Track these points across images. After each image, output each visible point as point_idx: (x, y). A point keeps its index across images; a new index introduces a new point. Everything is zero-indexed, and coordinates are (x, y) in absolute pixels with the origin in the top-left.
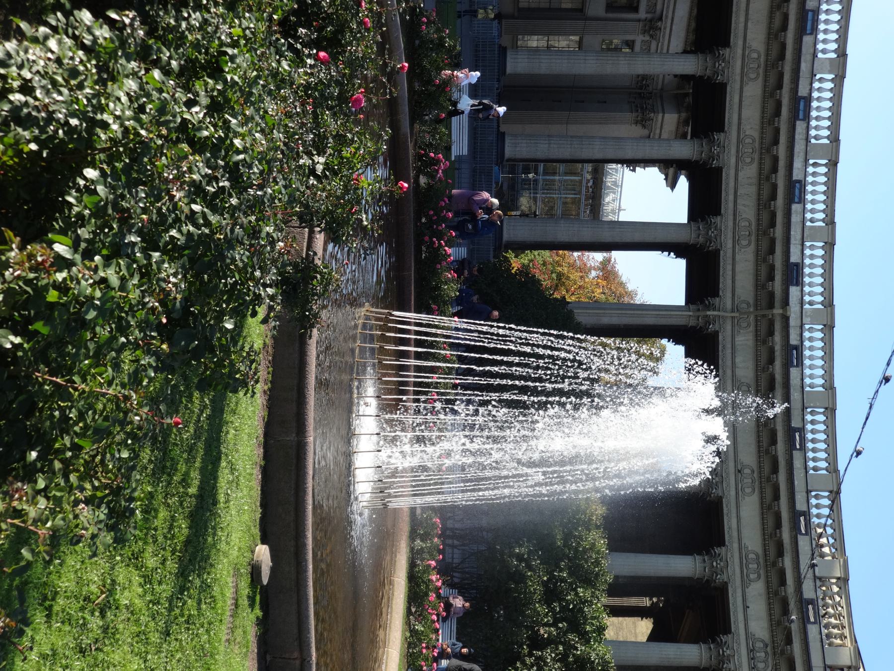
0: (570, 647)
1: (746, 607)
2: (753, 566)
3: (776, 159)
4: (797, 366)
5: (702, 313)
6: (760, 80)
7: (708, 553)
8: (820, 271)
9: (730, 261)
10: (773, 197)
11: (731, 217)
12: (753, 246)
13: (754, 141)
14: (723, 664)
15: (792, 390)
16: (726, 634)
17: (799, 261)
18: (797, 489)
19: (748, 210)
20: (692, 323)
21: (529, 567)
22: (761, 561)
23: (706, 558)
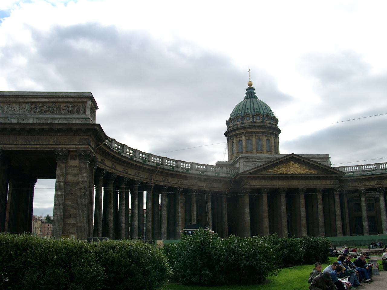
6: (383, 180)
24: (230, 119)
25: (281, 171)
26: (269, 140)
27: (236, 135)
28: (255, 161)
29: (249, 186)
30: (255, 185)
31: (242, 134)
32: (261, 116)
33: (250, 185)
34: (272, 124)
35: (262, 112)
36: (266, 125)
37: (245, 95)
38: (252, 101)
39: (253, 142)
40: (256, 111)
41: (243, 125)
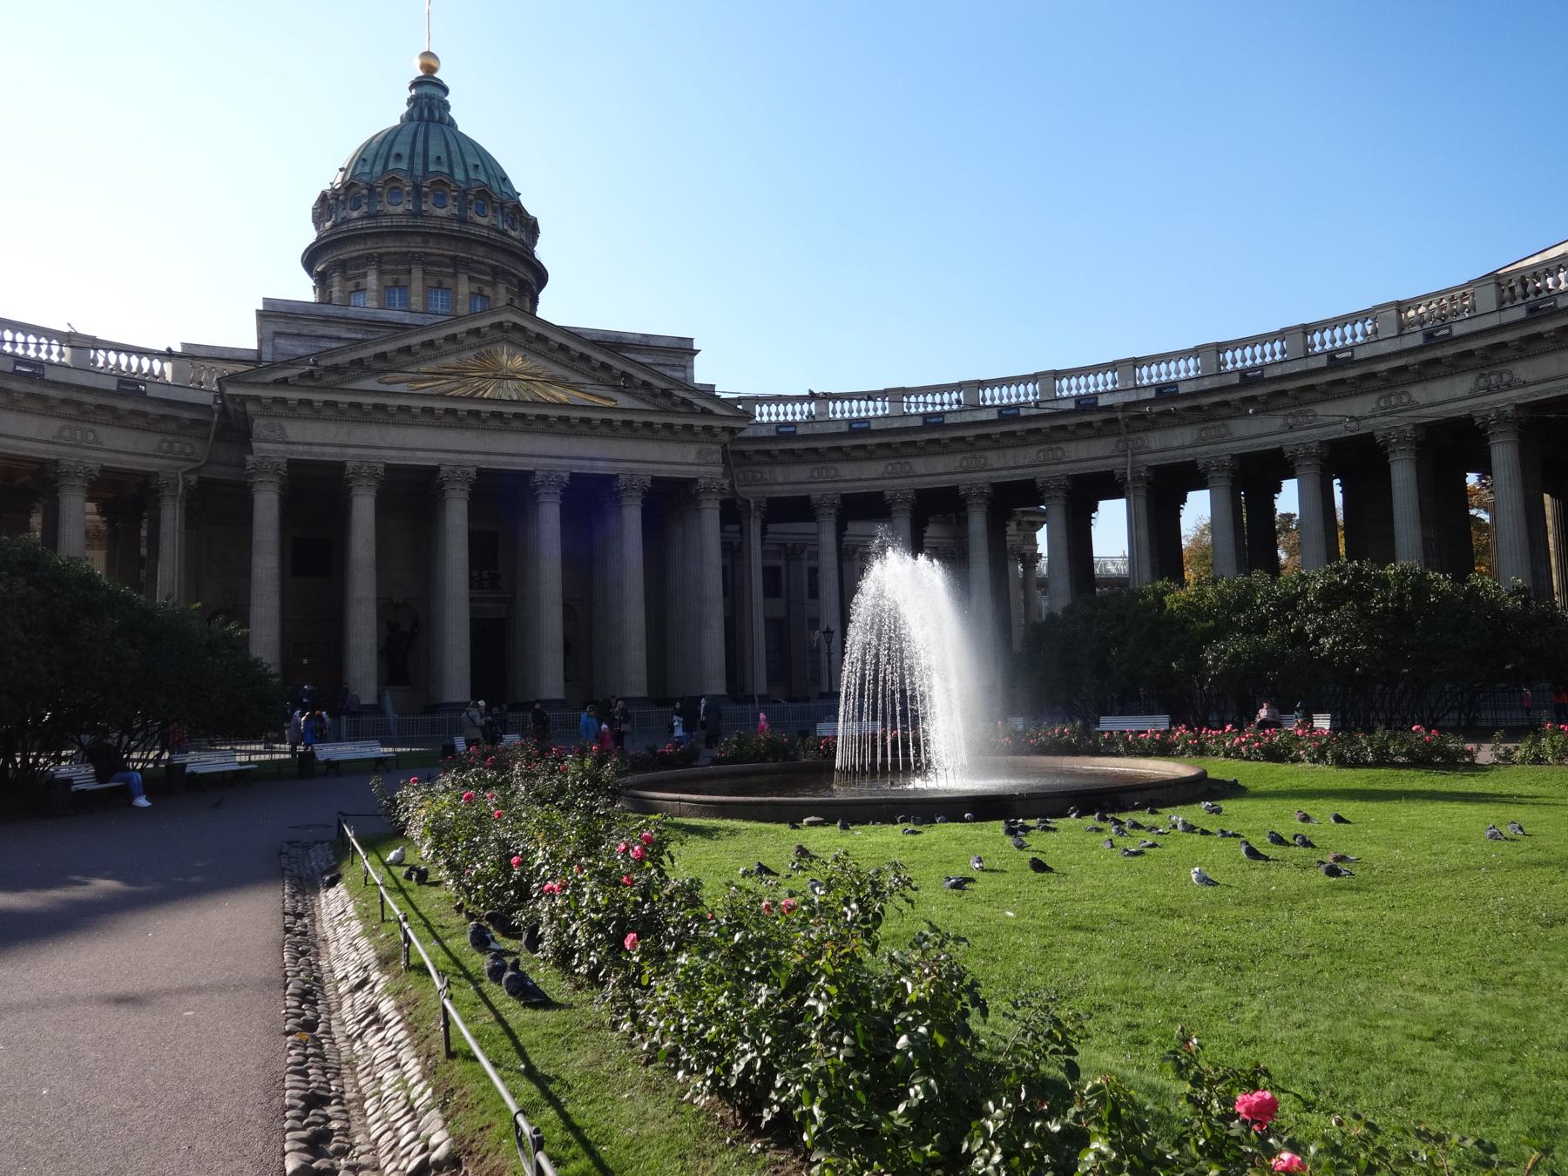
0: (1310, 608)
1: (1439, 404)
2: (1393, 400)
3: (978, 437)
4: (1177, 387)
5: (1131, 487)
6: (910, 460)
7: (1385, 448)
8: (1082, 380)
9: (1078, 465)
10: (1013, 433)
11: (1037, 469)
12: (1062, 445)
13: (965, 458)
14: (1507, 418)
15: (1202, 388)
16: (1472, 420)
17: (1073, 400)
18: (1304, 368)
19: (1028, 455)
20: (1142, 493)
21: (1225, 652)
22: (1386, 393)
23: (1390, 450)
24: (323, 197)
25: (455, 385)
26: (488, 297)
27: (342, 266)
28: (339, 339)
29: (282, 447)
30: (309, 444)
31: (366, 260)
32: (455, 194)
33: (289, 443)
34: (504, 233)
35: (459, 175)
36: (473, 230)
37: (405, 109)
38: (422, 129)
39: (413, 300)
40: (432, 168)
41: (372, 223)
